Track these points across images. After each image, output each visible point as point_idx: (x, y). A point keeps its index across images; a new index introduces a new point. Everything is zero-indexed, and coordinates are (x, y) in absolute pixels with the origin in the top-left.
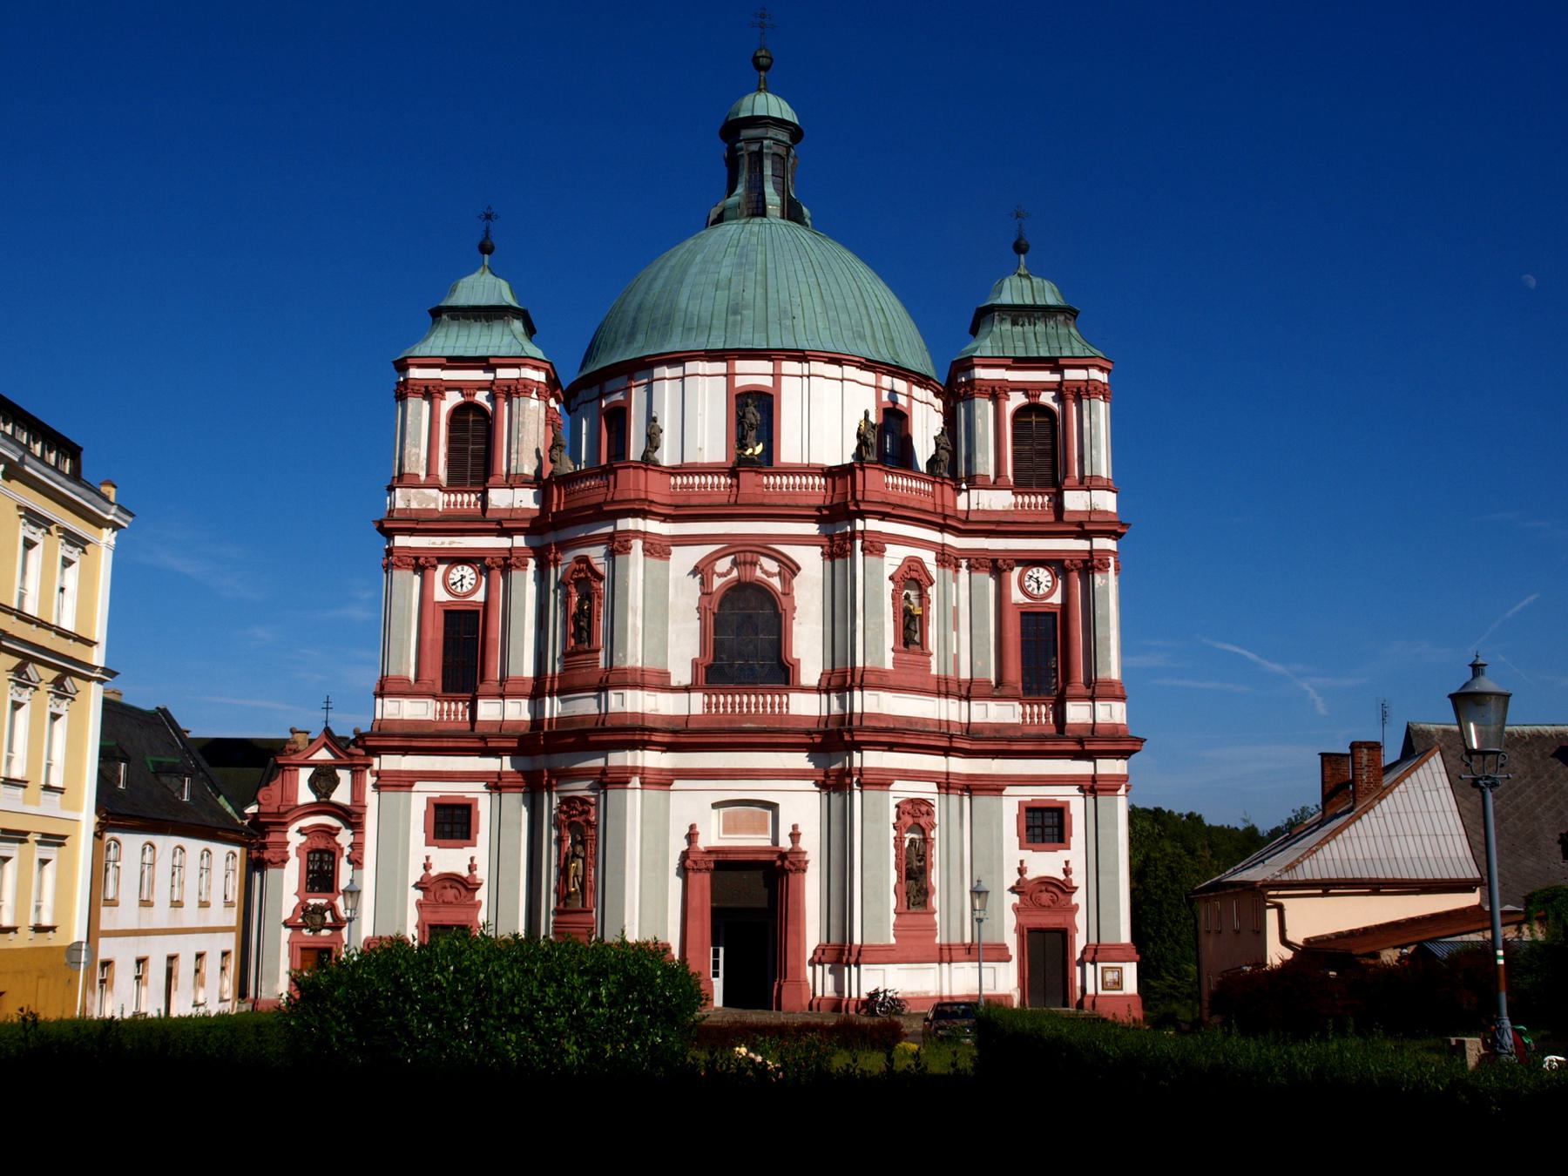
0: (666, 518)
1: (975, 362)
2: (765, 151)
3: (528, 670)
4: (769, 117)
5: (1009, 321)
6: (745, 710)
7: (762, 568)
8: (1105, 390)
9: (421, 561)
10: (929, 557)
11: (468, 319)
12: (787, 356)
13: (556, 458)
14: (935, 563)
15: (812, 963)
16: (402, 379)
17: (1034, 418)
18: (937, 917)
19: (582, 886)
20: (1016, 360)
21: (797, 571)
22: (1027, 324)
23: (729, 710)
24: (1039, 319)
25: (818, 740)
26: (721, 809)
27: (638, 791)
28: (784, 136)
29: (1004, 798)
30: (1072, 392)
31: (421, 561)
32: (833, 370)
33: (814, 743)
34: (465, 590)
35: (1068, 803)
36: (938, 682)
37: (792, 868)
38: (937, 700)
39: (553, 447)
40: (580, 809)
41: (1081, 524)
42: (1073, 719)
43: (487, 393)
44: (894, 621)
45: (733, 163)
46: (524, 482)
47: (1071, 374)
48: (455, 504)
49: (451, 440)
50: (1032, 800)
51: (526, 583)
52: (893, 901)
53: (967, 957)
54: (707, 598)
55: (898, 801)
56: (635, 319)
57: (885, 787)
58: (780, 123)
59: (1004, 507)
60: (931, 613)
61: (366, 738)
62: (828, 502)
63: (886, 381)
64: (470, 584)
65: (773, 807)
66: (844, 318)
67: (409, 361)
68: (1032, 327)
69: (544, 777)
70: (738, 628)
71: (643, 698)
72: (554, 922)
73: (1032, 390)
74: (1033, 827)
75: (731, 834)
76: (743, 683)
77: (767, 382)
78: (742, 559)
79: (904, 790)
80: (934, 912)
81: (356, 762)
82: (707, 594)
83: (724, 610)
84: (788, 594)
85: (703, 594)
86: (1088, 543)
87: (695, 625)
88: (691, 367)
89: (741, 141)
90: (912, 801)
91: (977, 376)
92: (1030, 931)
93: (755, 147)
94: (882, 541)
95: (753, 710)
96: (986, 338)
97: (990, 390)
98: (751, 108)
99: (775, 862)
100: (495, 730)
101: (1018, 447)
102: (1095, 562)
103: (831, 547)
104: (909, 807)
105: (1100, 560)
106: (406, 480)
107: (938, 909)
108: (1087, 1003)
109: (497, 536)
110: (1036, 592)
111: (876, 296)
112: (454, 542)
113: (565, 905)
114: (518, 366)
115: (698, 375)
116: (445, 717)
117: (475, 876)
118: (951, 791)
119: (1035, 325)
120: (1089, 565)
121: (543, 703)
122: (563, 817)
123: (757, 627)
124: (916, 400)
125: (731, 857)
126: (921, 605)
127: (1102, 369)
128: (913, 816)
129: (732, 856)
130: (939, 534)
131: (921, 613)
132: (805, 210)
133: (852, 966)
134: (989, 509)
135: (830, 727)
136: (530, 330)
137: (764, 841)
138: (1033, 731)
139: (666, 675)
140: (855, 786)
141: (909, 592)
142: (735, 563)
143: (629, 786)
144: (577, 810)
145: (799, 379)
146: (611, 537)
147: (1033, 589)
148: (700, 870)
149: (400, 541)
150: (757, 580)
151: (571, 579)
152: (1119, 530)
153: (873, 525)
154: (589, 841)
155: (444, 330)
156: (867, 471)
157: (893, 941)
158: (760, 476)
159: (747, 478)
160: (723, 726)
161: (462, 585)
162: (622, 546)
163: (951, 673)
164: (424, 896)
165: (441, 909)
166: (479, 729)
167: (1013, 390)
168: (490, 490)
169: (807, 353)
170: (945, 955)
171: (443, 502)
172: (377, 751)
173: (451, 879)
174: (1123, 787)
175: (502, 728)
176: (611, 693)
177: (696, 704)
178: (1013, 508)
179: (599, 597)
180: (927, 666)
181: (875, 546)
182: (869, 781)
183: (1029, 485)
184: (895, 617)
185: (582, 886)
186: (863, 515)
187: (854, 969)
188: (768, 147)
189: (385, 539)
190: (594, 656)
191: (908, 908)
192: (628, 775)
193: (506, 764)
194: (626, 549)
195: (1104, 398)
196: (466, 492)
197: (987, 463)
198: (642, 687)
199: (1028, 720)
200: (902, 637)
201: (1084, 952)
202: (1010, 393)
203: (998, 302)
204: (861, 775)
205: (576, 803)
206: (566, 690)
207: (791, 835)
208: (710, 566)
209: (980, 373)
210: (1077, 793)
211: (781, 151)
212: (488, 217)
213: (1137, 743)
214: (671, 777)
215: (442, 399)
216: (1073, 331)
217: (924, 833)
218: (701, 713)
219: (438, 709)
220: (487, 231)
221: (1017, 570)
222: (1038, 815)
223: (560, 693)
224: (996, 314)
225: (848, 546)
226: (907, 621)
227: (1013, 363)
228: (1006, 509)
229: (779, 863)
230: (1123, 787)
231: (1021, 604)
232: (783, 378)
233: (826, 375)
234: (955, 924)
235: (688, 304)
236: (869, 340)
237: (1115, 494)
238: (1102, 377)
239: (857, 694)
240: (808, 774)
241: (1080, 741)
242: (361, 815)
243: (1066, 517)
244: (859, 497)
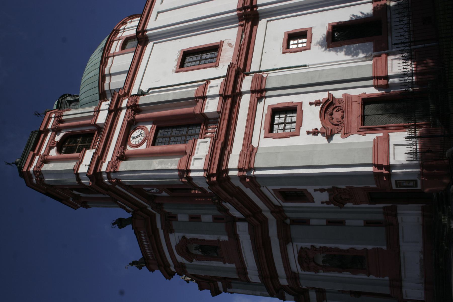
35: (269, 106)
110: (142, 138)
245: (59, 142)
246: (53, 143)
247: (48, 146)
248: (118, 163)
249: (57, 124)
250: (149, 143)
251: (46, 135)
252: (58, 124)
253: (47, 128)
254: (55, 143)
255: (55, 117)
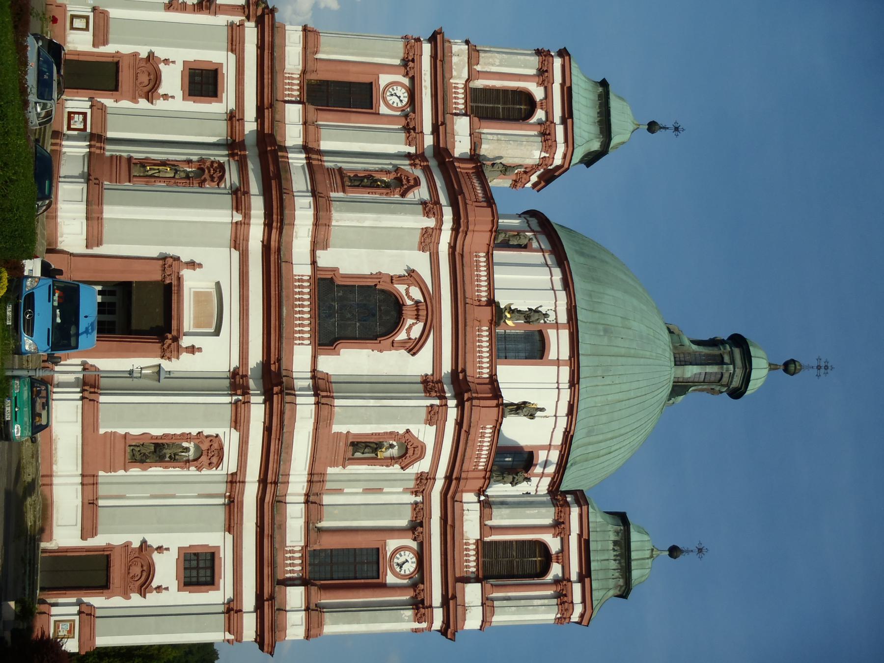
0: (453, 248)
1: (583, 507)
2: (725, 366)
3: (325, 145)
4: (751, 369)
5: (617, 538)
6: (297, 309)
7: (413, 324)
8: (565, 618)
9: (411, 64)
10: (423, 466)
11: (600, 107)
12: (574, 371)
13: (496, 168)
14: (419, 472)
15: (84, 364)
16: (553, 54)
17: (539, 559)
18: (121, 472)
19: (152, 176)
20: (587, 542)
21: (412, 353)
22: (615, 553)
23: (297, 296)
24: (620, 563)
25: (273, 368)
26: (215, 290)
27: (229, 220)
28: (736, 382)
29: (223, 533)
30: (563, 590)
31: (411, 64)
32: (563, 409)
33: (270, 364)
34: (388, 98)
35: (218, 589)
36: (321, 474)
37: (165, 346)
38: (306, 473)
39: (504, 165)
40: (215, 176)
41: (454, 597)
42: (289, 592)
43: (544, 119)
44: (372, 434)
45: (713, 343)
46: (475, 144)
47: (577, 588)
48: (456, 98)
49: (505, 92)
50: (220, 558)
51: (398, 146)
52: (135, 431)
53: (86, 501)
54: (389, 280)
55: (221, 436)
56: (595, 257)
57: (233, 424)
58: (747, 379)
59: (466, 532)
60: (377, 467)
61: (270, 15)
62: (469, 379)
63: (554, 456)
64: (394, 102)
65: (217, 333)
66: (604, 419)
67: (567, 58)
68: (613, 558)
69: (240, 151)
71: (306, 225)
72: (121, 157)
73: (563, 557)
74: (198, 560)
75: (194, 297)
76: (319, 309)
77: (552, 355)
78: (420, 308)
79: (231, 440)
80: (126, 470)
81: (251, 7)
82: (392, 280)
83: (379, 294)
84: (393, 346)
85: (392, 277)
86: (439, 605)
87: (366, 269)
88: (562, 296)
89: (731, 348)
90: (221, 449)
91: (572, 509)
92: (108, 556)
93: (727, 359)
94: (438, 422)
95: (298, 316)
96: (603, 519)
97: (561, 520)
98: (757, 356)
99: (170, 333)
100: (277, 117)
101: (514, 546)
102: (422, 610)
103: (433, 382)
104: (216, 446)
105: (424, 614)
106: (474, 54)
107: (128, 473)
108: (43, 608)
109: (432, 124)
110: (396, 560)
111: (620, 448)
112: (426, 89)
113: (135, 164)
114: (566, 141)
115: (556, 301)
116: (287, 81)
117: (159, 99)
118: (229, 485)
119: (615, 560)
120: (420, 606)
121: (301, 152)
122: (208, 164)
124: (540, 480)
125: (174, 297)
126: (386, 458)
127: (582, 616)
128: (208, 450)
129: (176, 297)
130: (444, 476)
131: (379, 457)
132: (680, 398)
133: (81, 394)
134: (464, 519)
135: (284, 379)
136: (590, 159)
137: (188, 324)
138: (279, 559)
139: (325, 247)
140: (235, 398)
141: (396, 448)
142: (417, 303)
143: (235, 212)
144: (214, 173)
145: (556, 381)
146: (437, 202)
147: (398, 559)
148: (164, 270)
149: (427, 48)
150: (404, 319)
151: (401, 175)
152: (449, 631)
153: (452, 414)
154: (188, 181)
155: (590, 88)
156: (496, 409)
157: (102, 431)
158: (488, 324)
159: (486, 313)
160: (284, 291)
162: (430, 211)
163: (328, 486)
164: (142, 59)
165: (131, 71)
166: (278, 105)
167: (562, 540)
168: (468, 118)
169: (577, 386)
170: (89, 481)
171: (457, 84)
172: (260, 22)
173: (156, 80)
174: (232, 637)
175: (278, 122)
176: (311, 199)
177: (301, 268)
178: (464, 541)
179: (387, 193)
180: (334, 464)
181: (434, 417)
182: (239, 409)
183: (484, 556)
184: (376, 434)
185: (152, 176)
186: (460, 405)
187: (79, 396)
188: (727, 370)
189: (428, 38)
190: (340, 188)
191: (130, 446)
192: (243, 211)
193: (250, 126)
194: (427, 214)
195: (559, 618)
196: (466, 101)
197: (502, 518)
198: (316, 224)
199: (288, 555)
200: (359, 440)
201: (89, 605)
202: (559, 538)
203: (632, 530)
204: (244, 403)
205: (220, 172)
206: (312, 169)
207: (193, 346)
208: (415, 283)
209: (575, 512)
210: (227, 597)
211: (725, 380)
212: (677, 129)
213: (270, 648)
214: (241, 249)
215: (537, 83)
216: (611, 593)
217: (194, 460)
218: (294, 273)
219: (294, 76)
220: (665, 128)
221: (414, 545)
222: (208, 564)
223: (310, 165)
224: (622, 528)
225: (434, 394)
226: (372, 445)
227: (585, 539)
228: (465, 534)
229: (170, 336)
230: (232, 637)
231: (385, 548)
232: (556, 367)
233: (559, 402)
234: (115, 490)
235: (610, 295)
236: (587, 440)
237: (479, 628)
238: (575, 617)
239: (312, 400)
240: (244, 360)
241: (272, 598)
242: (208, 8)
243: (459, 585)
244: (475, 402)
250: (384, 552)
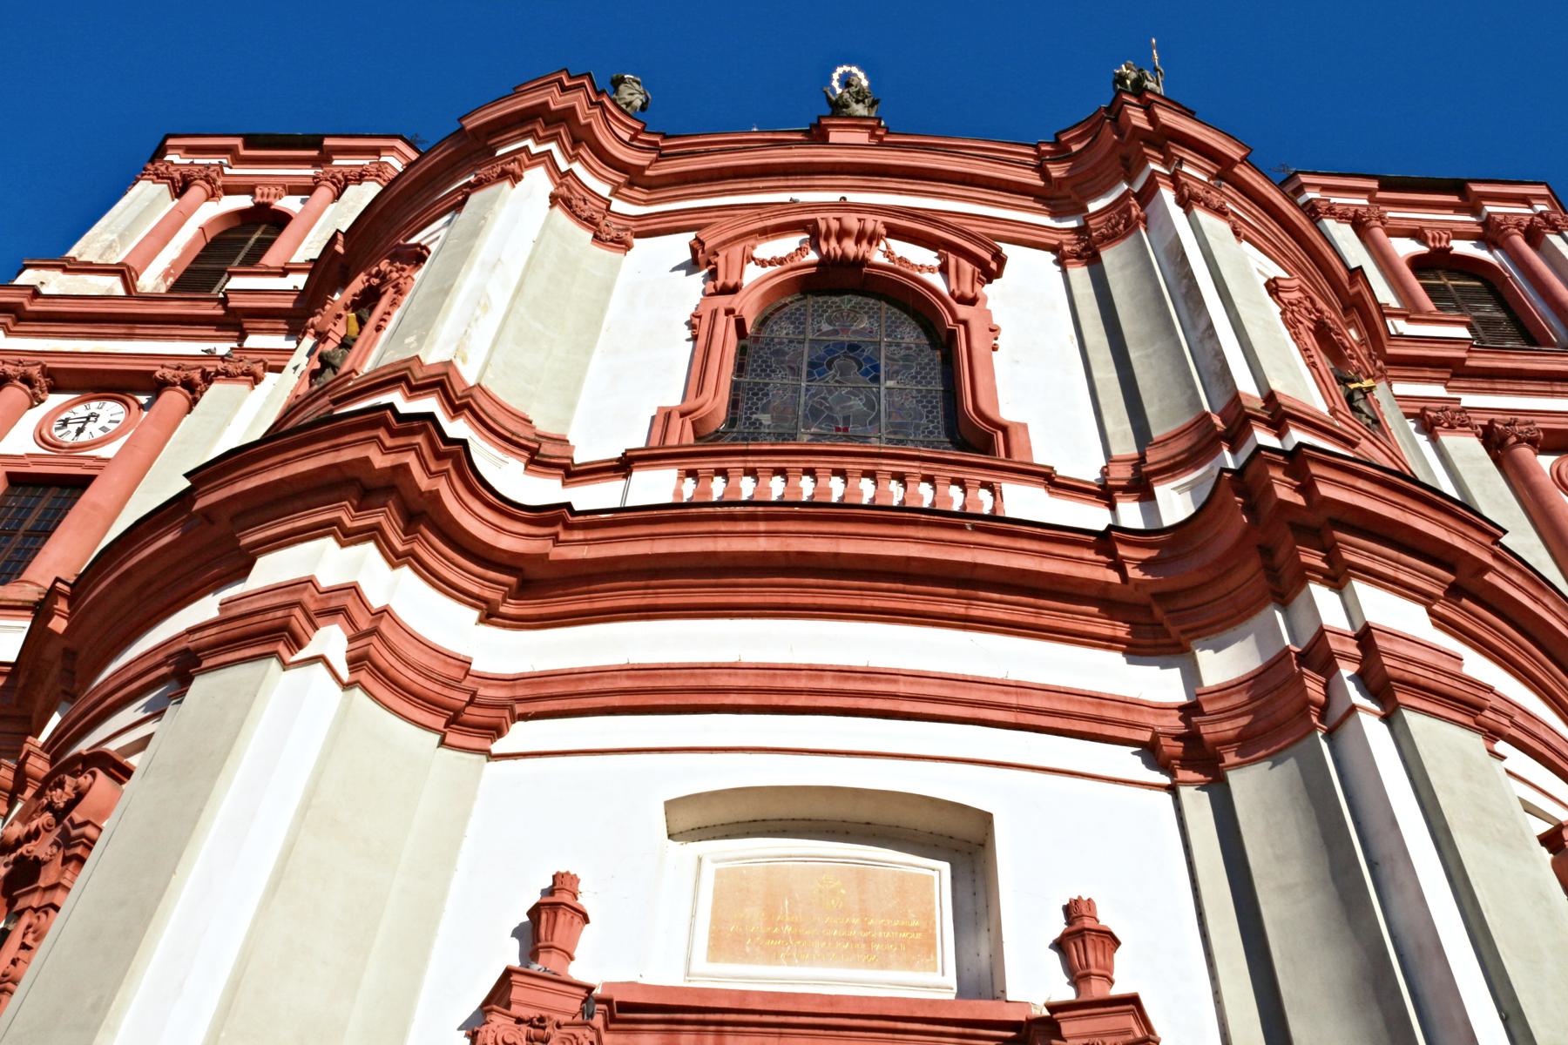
34: (84, 437)
70: (812, 365)
123: (876, 368)
161: (80, 431)
245: (1452, 252)
246: (1437, 236)
247: (1423, 224)
248: (1468, 429)
249: (1518, 225)
251: (1457, 209)
252: (1520, 230)
253: (1484, 203)
254: (1440, 242)
255: (1541, 214)
